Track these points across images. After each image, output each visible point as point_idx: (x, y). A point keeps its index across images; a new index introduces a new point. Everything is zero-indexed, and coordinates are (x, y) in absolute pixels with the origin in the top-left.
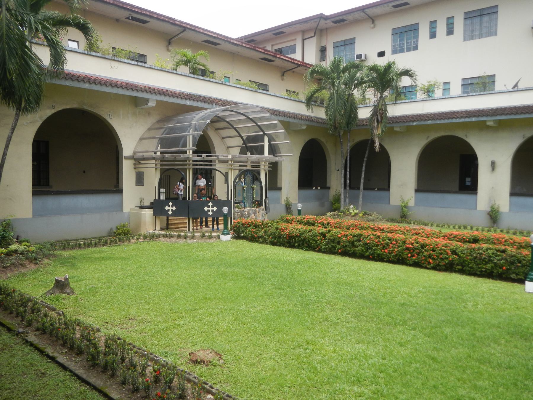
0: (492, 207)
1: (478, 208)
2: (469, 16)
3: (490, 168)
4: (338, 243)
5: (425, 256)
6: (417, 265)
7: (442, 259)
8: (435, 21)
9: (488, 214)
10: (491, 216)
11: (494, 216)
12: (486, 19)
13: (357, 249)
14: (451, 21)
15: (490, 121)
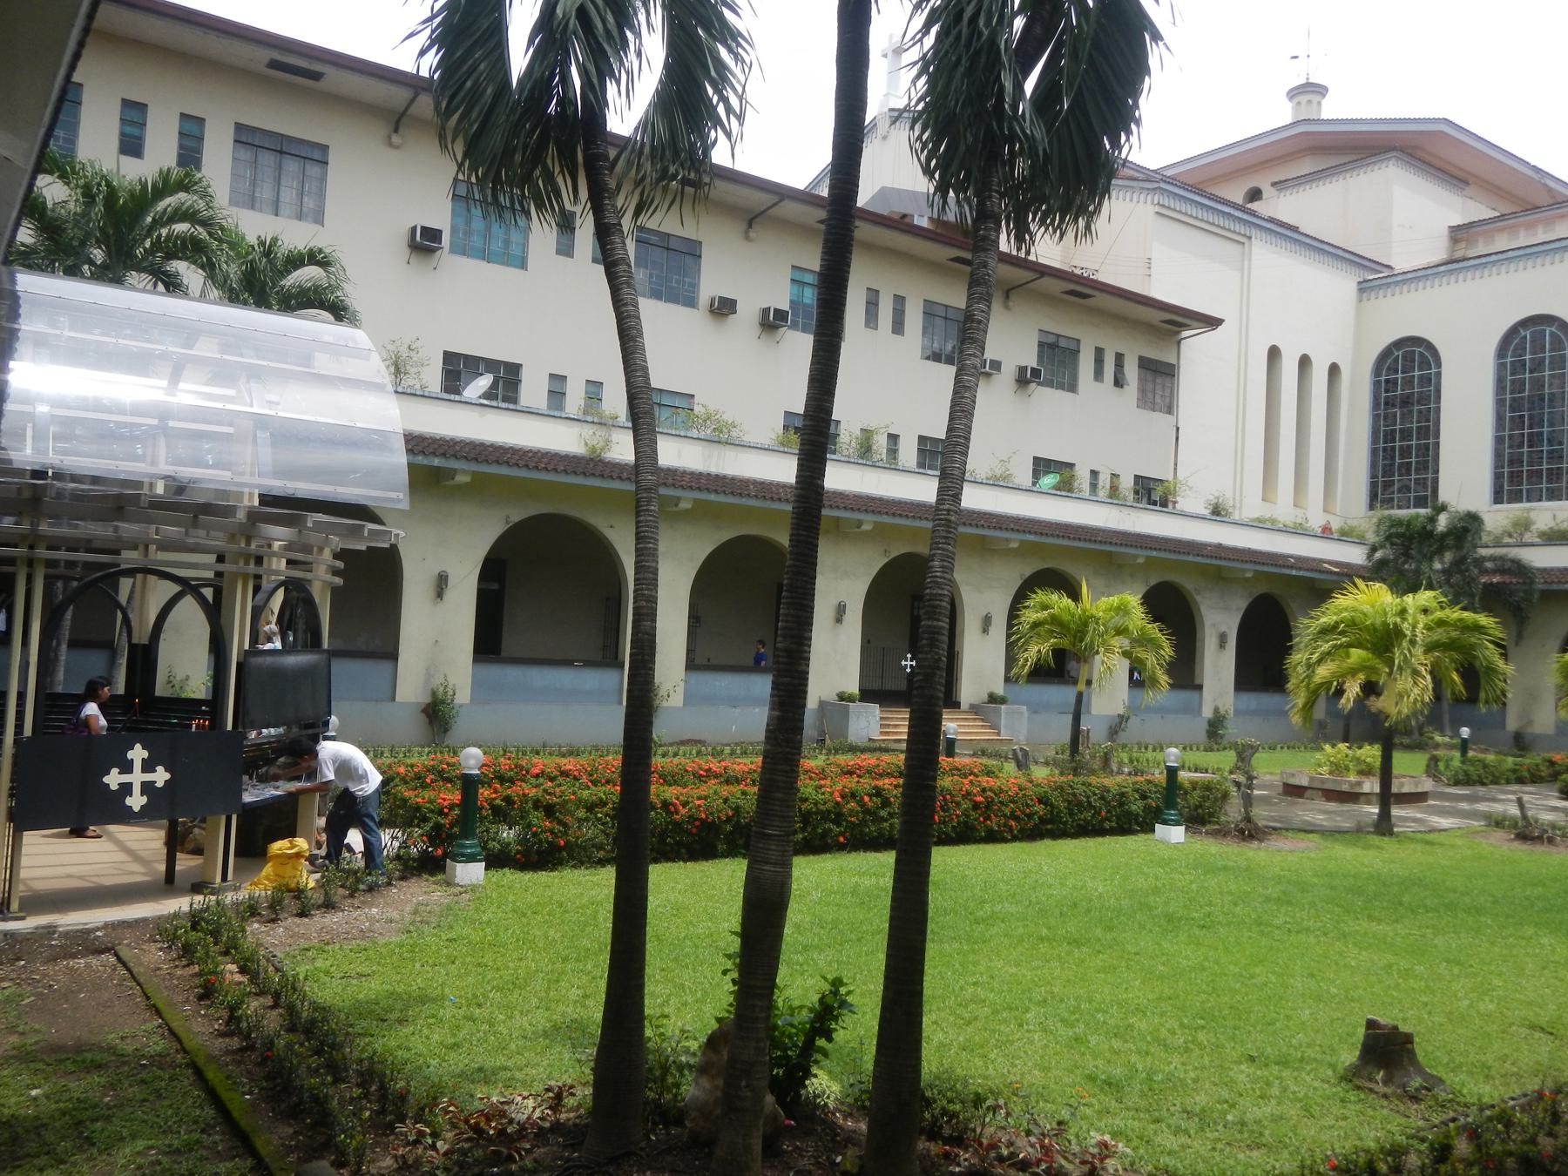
0: (434, 693)
1: (398, 699)
2: (246, 137)
3: (432, 594)
4: (838, 818)
5: (1004, 816)
6: (992, 837)
7: (1029, 816)
8: (142, 107)
9: (425, 711)
10: (428, 716)
11: (436, 714)
12: (291, 166)
13: (886, 825)
14: (191, 128)
15: (464, 472)
